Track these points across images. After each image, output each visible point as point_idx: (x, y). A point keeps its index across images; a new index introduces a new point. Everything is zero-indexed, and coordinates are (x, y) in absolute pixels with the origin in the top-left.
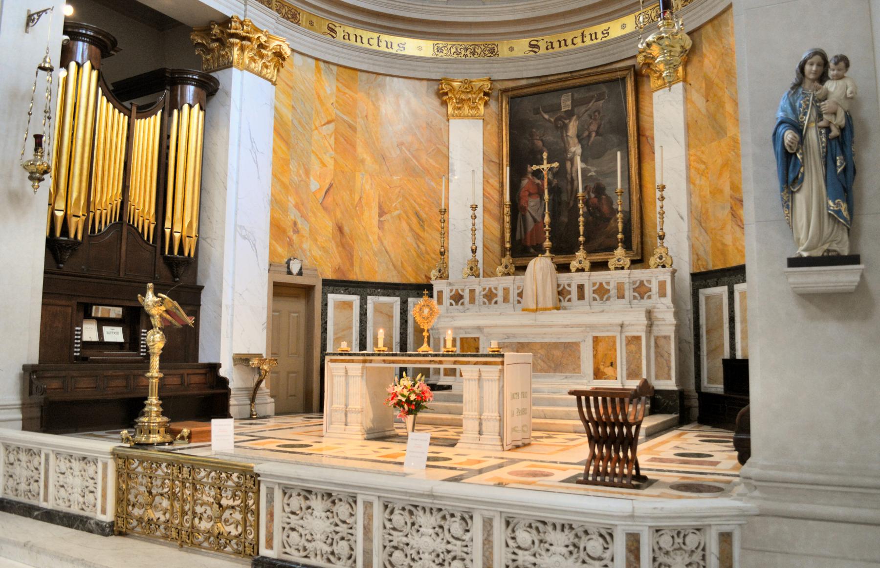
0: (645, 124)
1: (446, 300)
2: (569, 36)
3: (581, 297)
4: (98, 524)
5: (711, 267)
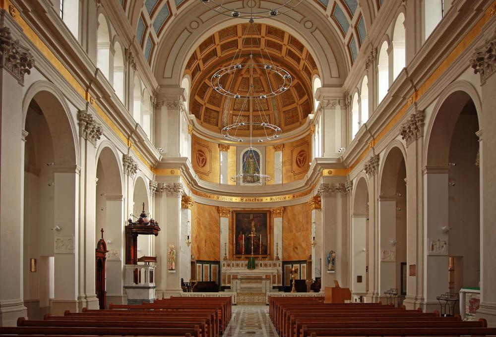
0: (272, 225)
2: (252, 199)
3: (261, 266)
5: (287, 260)
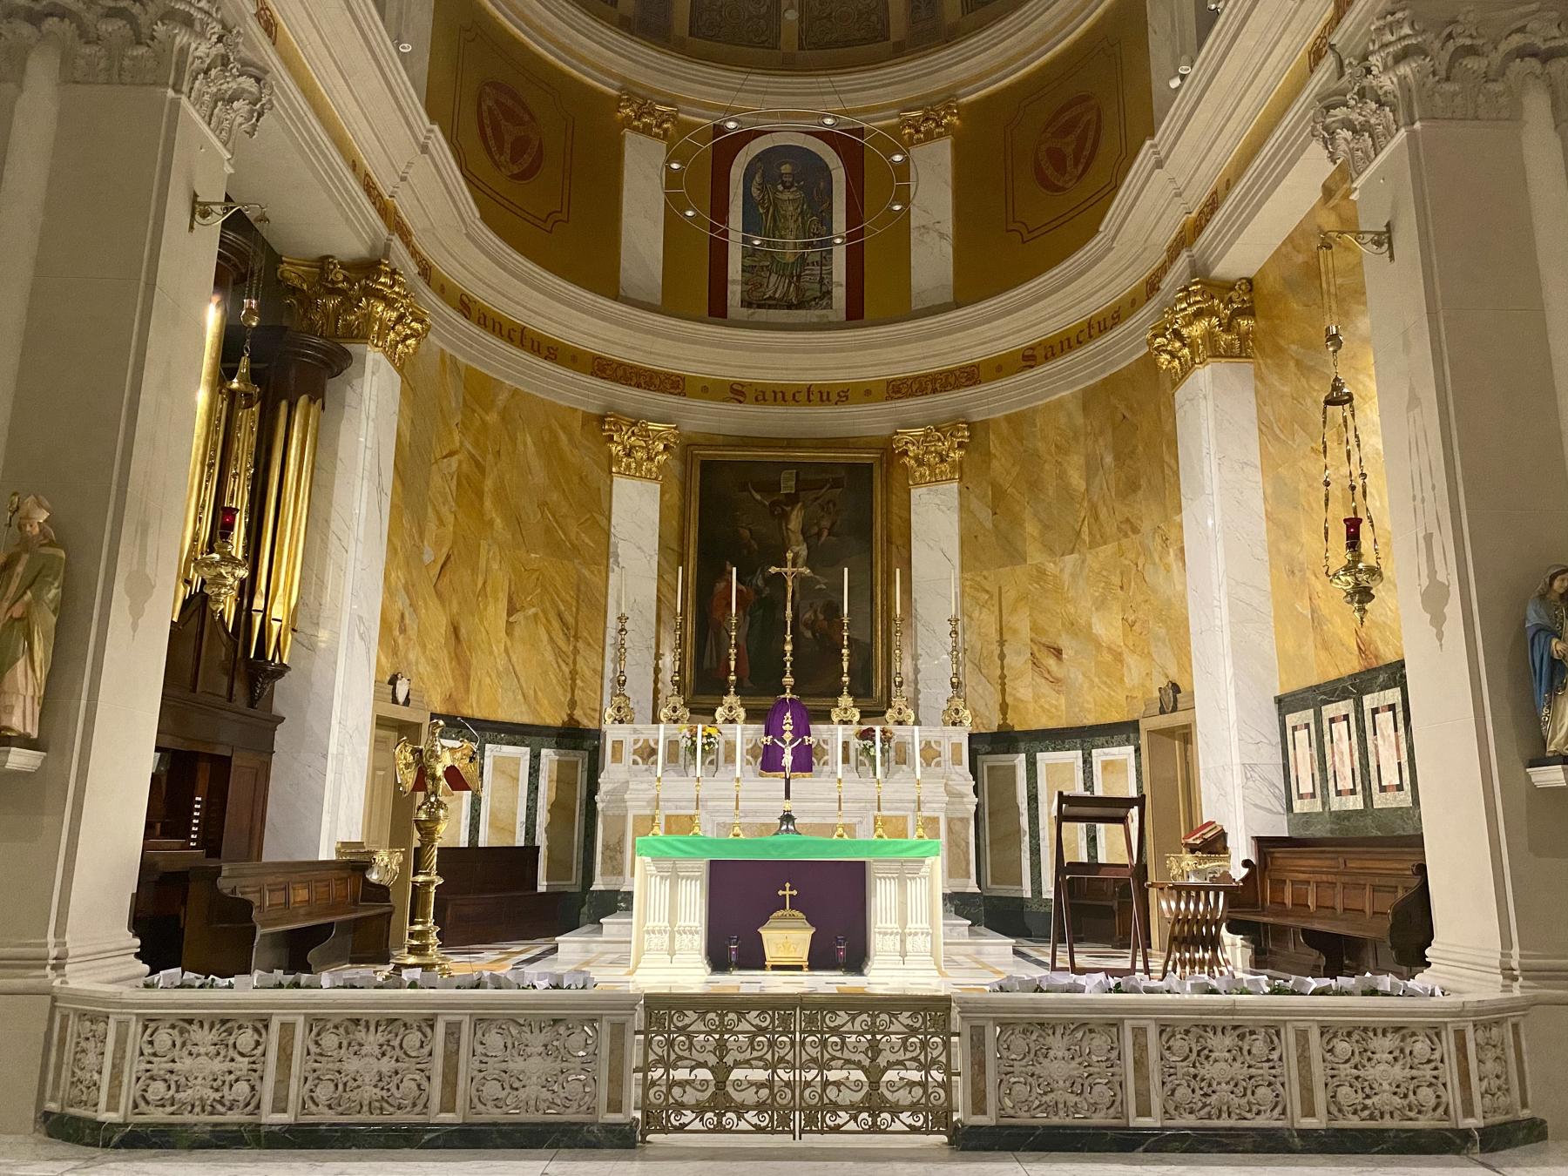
1: (628, 755)
4: (1304, 1134)
